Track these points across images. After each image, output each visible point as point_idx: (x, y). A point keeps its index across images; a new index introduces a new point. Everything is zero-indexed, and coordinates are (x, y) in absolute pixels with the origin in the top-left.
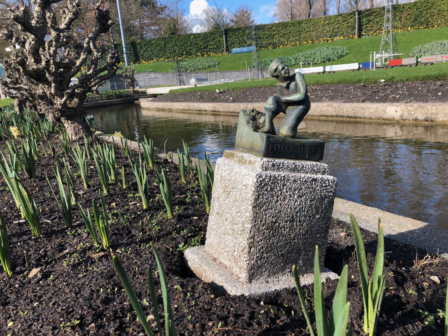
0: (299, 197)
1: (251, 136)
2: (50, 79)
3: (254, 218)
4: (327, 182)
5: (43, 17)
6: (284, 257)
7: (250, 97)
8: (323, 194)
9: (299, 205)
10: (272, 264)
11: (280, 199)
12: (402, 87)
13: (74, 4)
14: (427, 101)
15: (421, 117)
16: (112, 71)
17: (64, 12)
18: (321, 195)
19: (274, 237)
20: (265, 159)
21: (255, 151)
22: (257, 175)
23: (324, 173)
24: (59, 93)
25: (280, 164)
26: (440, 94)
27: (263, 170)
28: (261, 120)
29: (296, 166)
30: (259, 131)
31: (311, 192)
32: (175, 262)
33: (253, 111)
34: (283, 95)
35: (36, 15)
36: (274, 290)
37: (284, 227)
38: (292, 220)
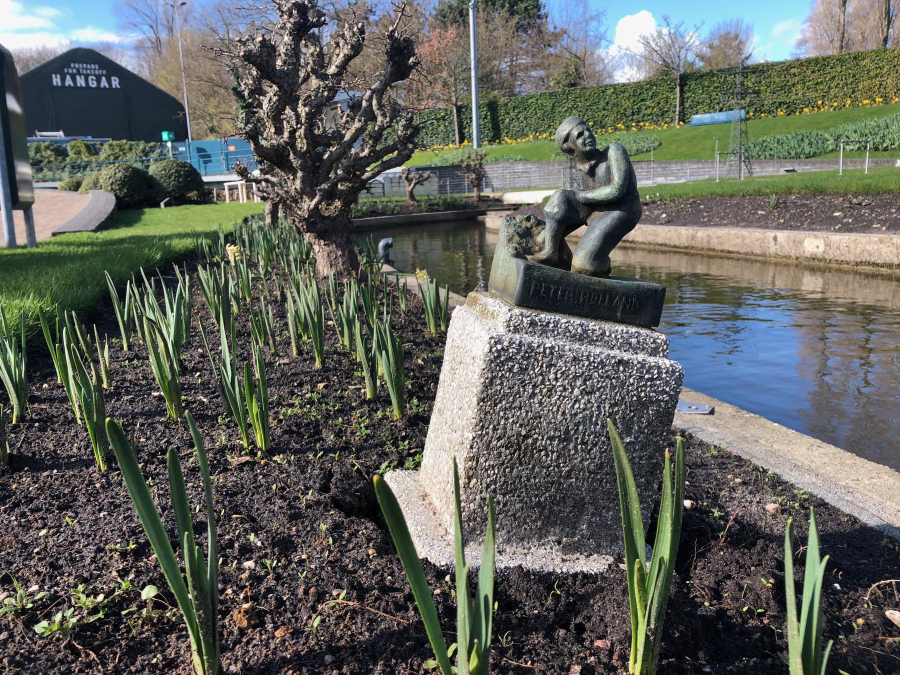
0: (584, 392)
2: (295, 162)
3: (481, 421)
4: (656, 371)
5: (295, 52)
6: (544, 508)
7: (705, 214)
8: (643, 394)
9: (584, 410)
10: (515, 519)
11: (541, 391)
13: (355, 29)
16: (404, 153)
17: (338, 44)
18: (639, 397)
19: (521, 464)
20: (517, 311)
22: (492, 338)
23: (654, 352)
24: (308, 190)
25: (549, 323)
27: (510, 331)
28: (539, 239)
29: (585, 331)
30: (529, 257)
31: (613, 387)
32: (357, 491)
35: (284, 50)
36: (503, 567)
37: (545, 449)
38: (566, 438)
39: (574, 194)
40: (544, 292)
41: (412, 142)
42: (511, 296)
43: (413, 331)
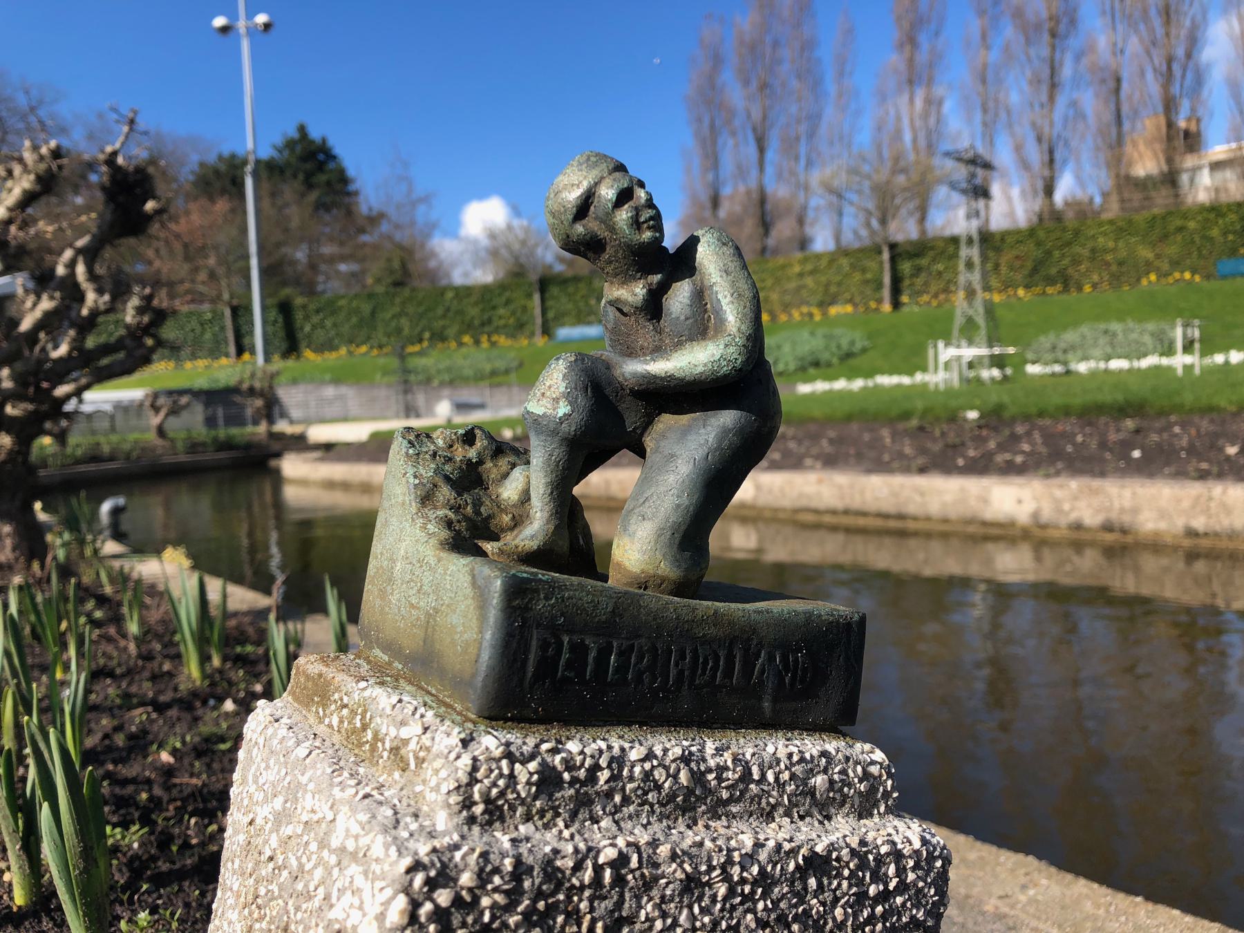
1: (427, 578)
4: (892, 870)
12: (1028, 434)
13: (44, 150)
14: (1103, 474)
15: (1090, 517)
20: (490, 742)
21: (442, 673)
22: (411, 870)
25: (596, 768)
26: (1136, 454)
27: (471, 820)
28: (509, 491)
29: (698, 777)
30: (489, 547)
33: (469, 438)
34: (631, 352)
39: (608, 366)
40: (569, 665)
41: (154, 336)
42: (459, 684)
43: (154, 678)
